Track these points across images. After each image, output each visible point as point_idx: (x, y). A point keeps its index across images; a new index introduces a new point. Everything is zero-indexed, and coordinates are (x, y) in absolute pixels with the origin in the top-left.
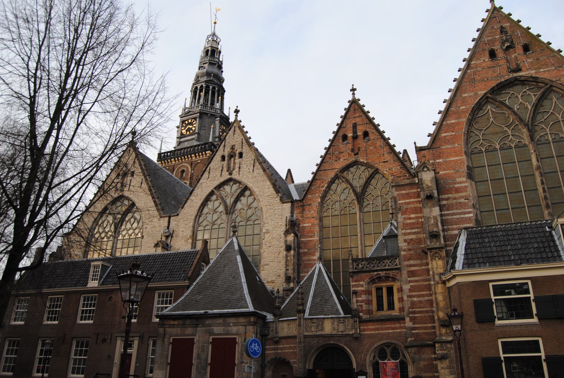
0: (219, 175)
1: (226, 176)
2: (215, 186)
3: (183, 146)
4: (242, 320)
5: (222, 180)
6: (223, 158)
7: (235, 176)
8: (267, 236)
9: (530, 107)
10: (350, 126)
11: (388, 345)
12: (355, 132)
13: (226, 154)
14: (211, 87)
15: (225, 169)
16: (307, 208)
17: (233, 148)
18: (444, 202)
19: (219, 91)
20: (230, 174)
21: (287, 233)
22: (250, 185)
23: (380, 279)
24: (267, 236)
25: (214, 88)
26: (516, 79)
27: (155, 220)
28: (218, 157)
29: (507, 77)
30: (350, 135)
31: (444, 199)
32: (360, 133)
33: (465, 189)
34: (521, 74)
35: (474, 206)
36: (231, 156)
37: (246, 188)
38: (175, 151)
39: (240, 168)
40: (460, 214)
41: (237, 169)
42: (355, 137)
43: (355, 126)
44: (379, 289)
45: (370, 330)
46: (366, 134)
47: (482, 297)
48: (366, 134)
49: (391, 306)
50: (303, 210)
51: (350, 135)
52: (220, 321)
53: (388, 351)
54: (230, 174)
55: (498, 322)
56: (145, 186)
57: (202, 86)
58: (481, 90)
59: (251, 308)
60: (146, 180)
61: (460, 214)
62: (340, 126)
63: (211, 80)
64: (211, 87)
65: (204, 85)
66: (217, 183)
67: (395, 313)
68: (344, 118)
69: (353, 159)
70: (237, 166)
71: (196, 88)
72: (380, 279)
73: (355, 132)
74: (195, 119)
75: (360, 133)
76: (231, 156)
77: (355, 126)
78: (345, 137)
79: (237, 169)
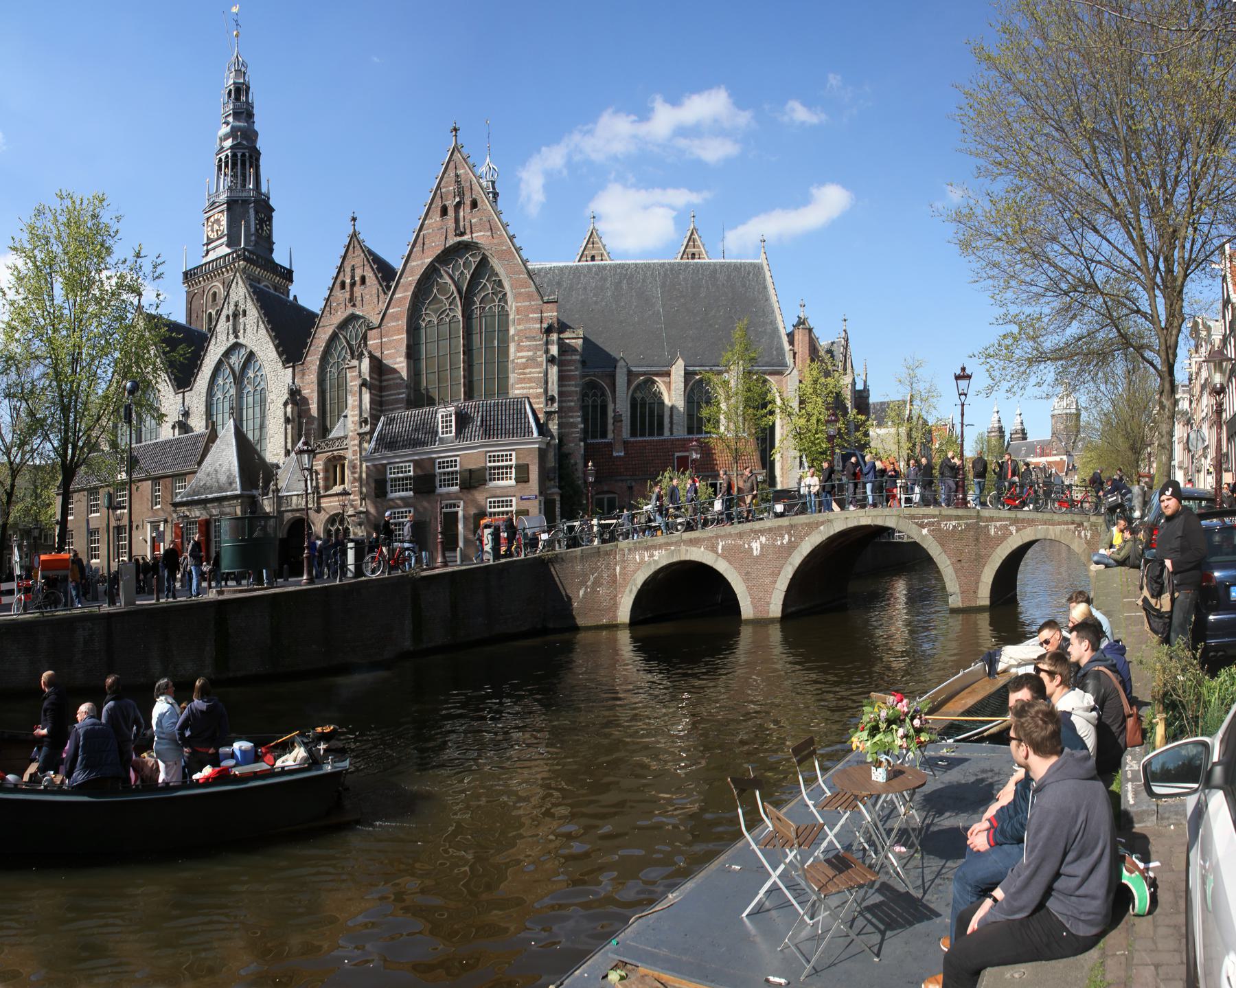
0: (225, 339)
1: (232, 340)
5: (229, 345)
6: (228, 317)
7: (241, 340)
8: (272, 406)
9: (468, 277)
10: (348, 270)
12: (353, 277)
13: (231, 313)
15: (231, 331)
16: (307, 372)
18: (385, 383)
21: (285, 404)
22: (254, 349)
24: (272, 406)
27: (171, 397)
28: (223, 318)
30: (348, 281)
31: (385, 380)
32: (357, 279)
35: (407, 387)
37: (251, 355)
39: (244, 329)
40: (395, 394)
41: (242, 331)
42: (353, 284)
43: (353, 269)
49: (343, 482)
50: (304, 375)
51: (348, 281)
61: (395, 394)
62: (341, 269)
66: (224, 349)
68: (344, 258)
70: (242, 327)
73: (353, 277)
75: (357, 279)
76: (235, 315)
77: (353, 269)
79: (242, 331)
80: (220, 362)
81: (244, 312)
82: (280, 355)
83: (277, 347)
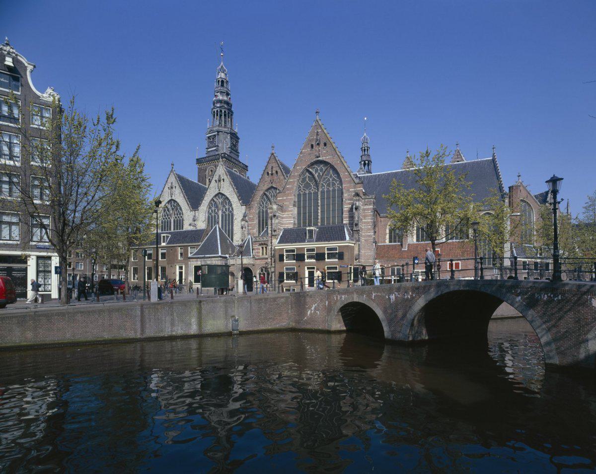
1: (217, 192)
2: (213, 196)
3: (211, 154)
4: (217, 259)
6: (216, 181)
11: (264, 267)
12: (272, 171)
14: (223, 111)
17: (220, 176)
19: (229, 113)
20: (219, 190)
22: (228, 196)
23: (262, 244)
25: (225, 112)
26: (318, 161)
29: (314, 160)
30: (270, 173)
33: (291, 211)
34: (319, 159)
36: (220, 181)
37: (227, 198)
38: (206, 158)
42: (272, 174)
43: (272, 168)
44: (263, 248)
45: (258, 262)
46: (277, 172)
47: (281, 253)
48: (277, 172)
49: (266, 254)
50: (250, 209)
52: (209, 259)
53: (264, 269)
54: (219, 190)
55: (285, 261)
56: (181, 194)
57: (217, 111)
58: (304, 165)
59: (220, 254)
60: (182, 192)
63: (222, 106)
64: (223, 111)
65: (219, 110)
66: (214, 194)
67: (267, 256)
69: (270, 185)
71: (214, 112)
72: (262, 244)
73: (272, 171)
74: (215, 135)
77: (272, 168)
78: (268, 173)
79: (222, 188)
80: (212, 200)
81: (223, 180)
82: (239, 200)
83: (238, 197)
